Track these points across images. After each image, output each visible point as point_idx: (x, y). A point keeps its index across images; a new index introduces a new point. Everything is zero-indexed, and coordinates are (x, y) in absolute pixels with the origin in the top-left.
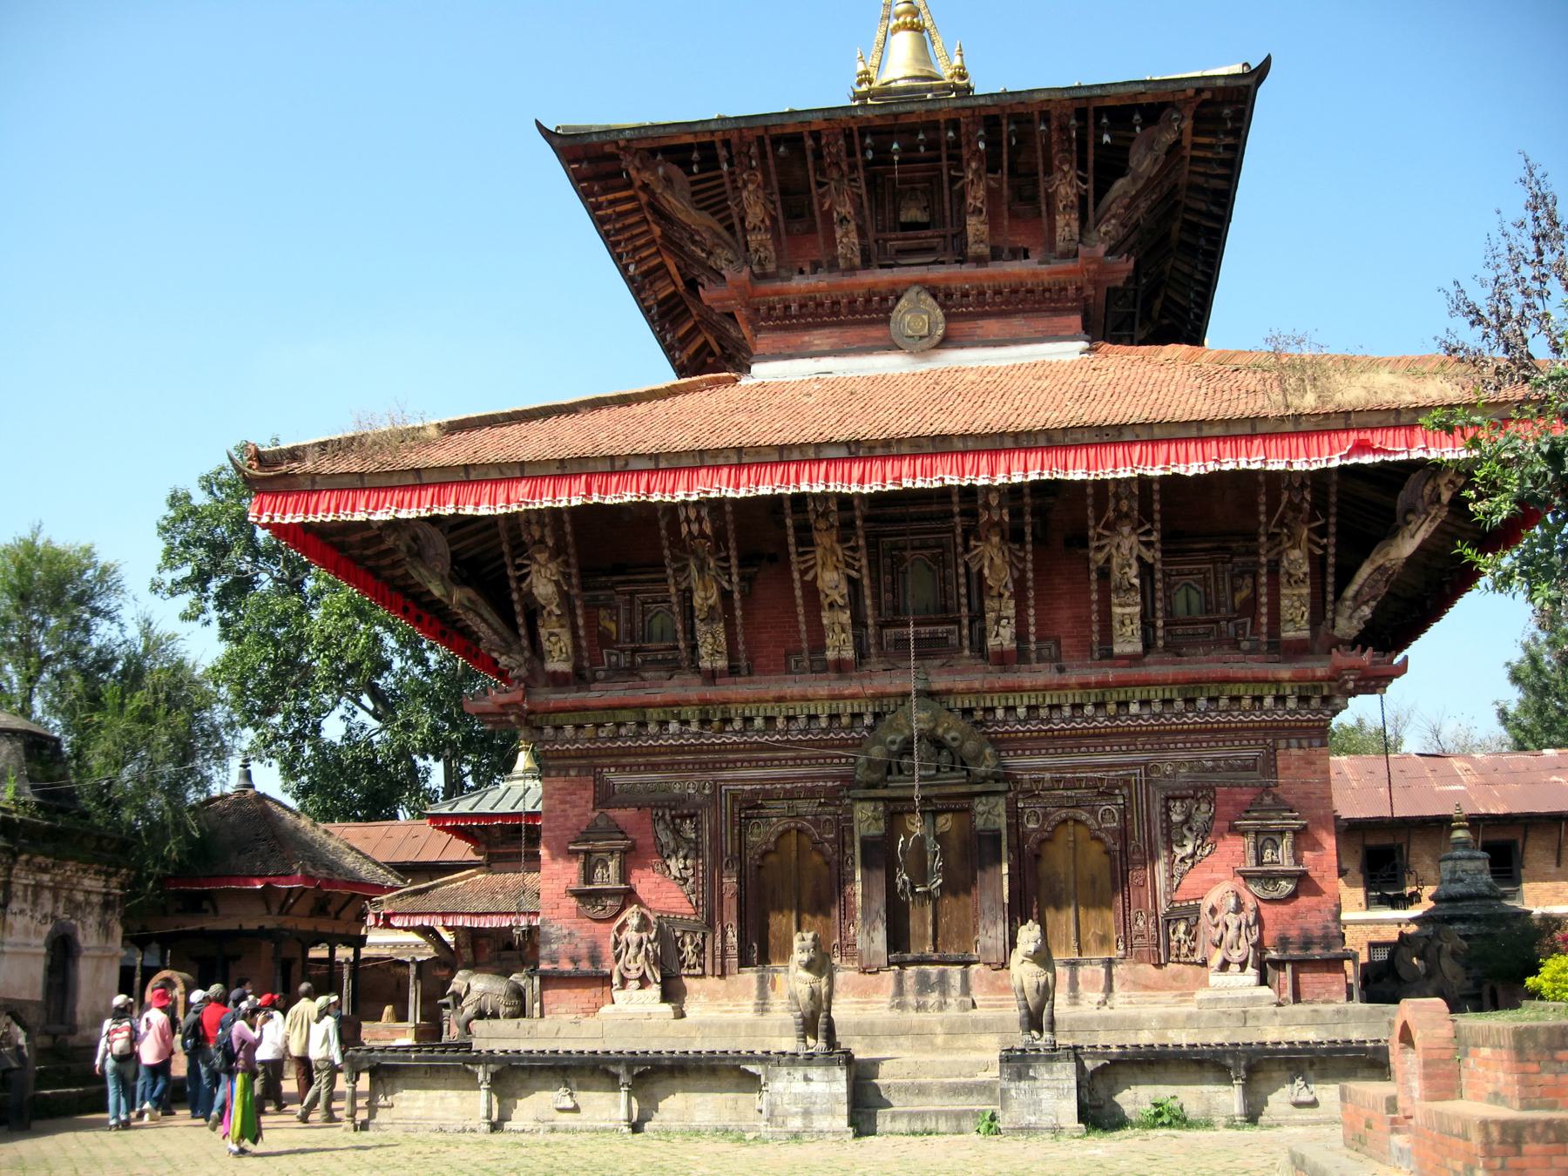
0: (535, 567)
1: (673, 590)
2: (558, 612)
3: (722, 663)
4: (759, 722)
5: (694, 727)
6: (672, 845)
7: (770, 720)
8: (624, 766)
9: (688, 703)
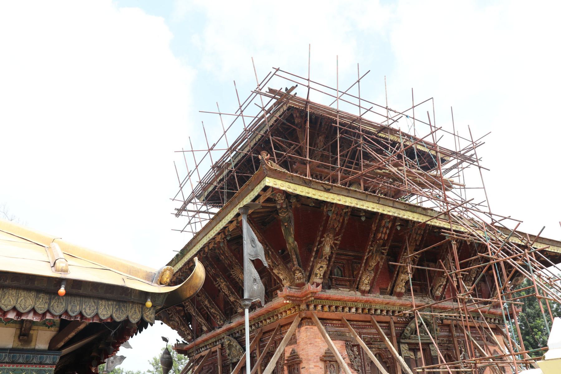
0: (328, 239)
1: (365, 258)
2: (328, 258)
3: (368, 288)
4: (379, 311)
5: (360, 311)
6: (353, 356)
7: (382, 311)
8: (334, 324)
9: (361, 301)
